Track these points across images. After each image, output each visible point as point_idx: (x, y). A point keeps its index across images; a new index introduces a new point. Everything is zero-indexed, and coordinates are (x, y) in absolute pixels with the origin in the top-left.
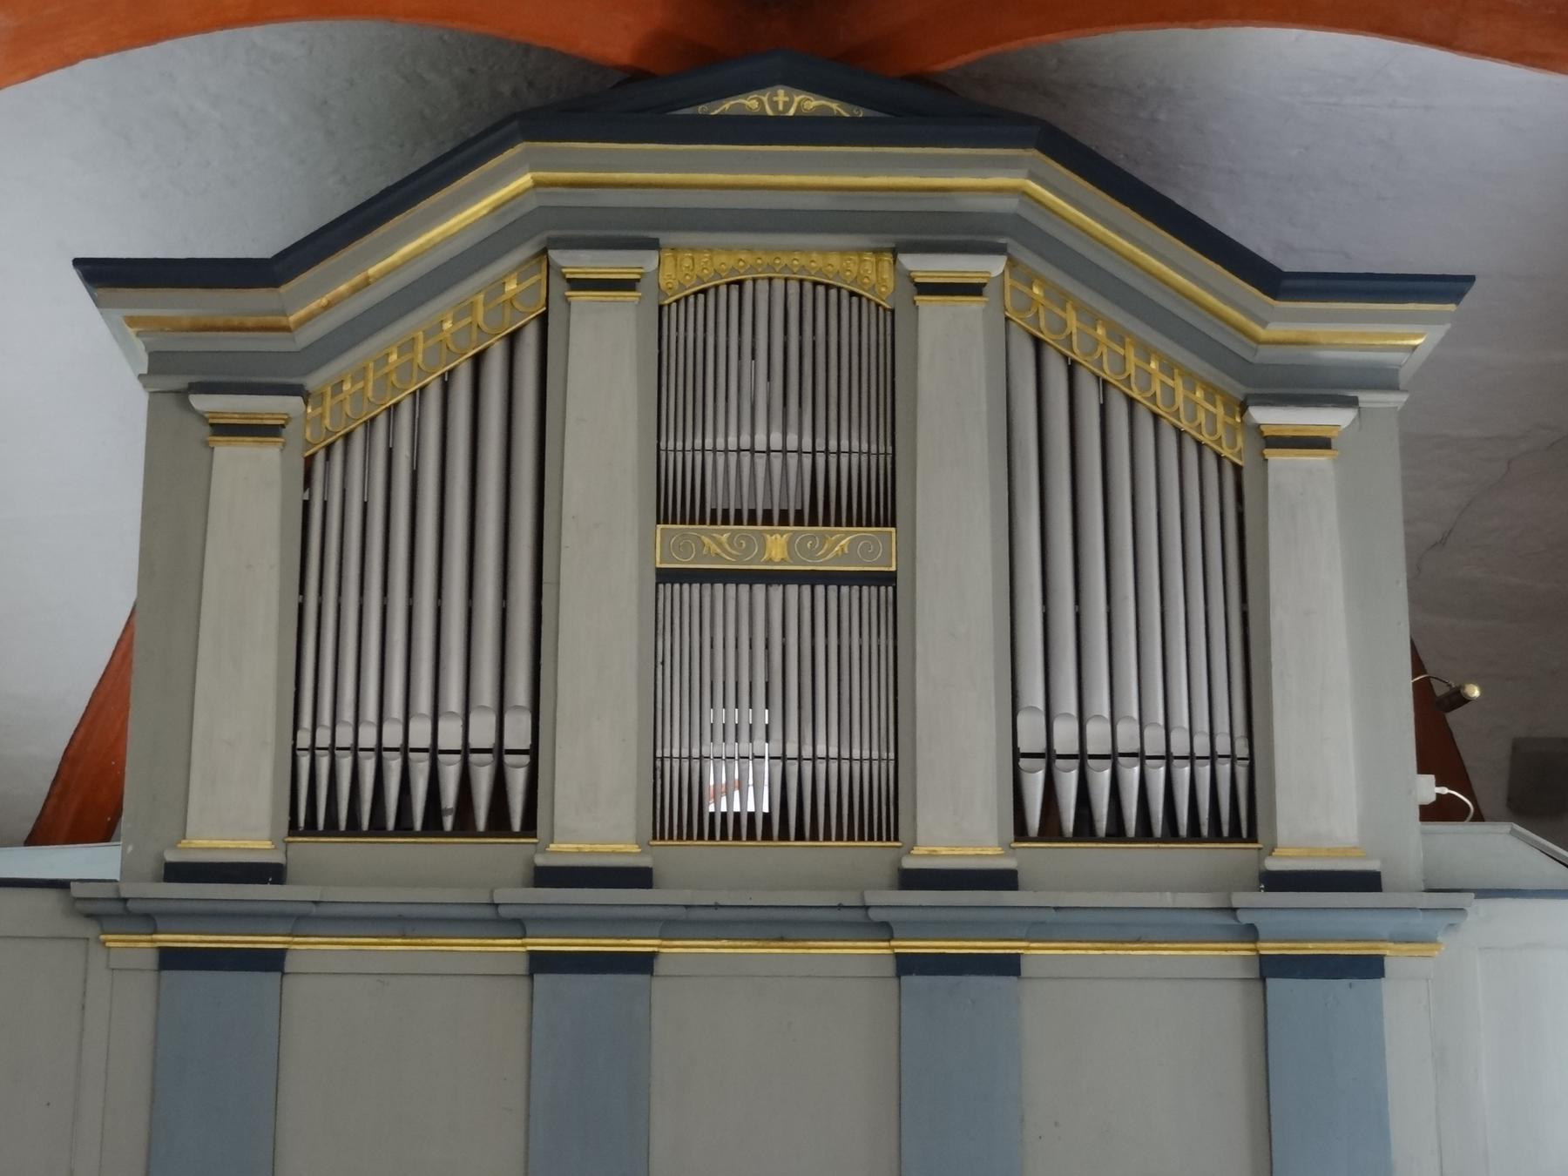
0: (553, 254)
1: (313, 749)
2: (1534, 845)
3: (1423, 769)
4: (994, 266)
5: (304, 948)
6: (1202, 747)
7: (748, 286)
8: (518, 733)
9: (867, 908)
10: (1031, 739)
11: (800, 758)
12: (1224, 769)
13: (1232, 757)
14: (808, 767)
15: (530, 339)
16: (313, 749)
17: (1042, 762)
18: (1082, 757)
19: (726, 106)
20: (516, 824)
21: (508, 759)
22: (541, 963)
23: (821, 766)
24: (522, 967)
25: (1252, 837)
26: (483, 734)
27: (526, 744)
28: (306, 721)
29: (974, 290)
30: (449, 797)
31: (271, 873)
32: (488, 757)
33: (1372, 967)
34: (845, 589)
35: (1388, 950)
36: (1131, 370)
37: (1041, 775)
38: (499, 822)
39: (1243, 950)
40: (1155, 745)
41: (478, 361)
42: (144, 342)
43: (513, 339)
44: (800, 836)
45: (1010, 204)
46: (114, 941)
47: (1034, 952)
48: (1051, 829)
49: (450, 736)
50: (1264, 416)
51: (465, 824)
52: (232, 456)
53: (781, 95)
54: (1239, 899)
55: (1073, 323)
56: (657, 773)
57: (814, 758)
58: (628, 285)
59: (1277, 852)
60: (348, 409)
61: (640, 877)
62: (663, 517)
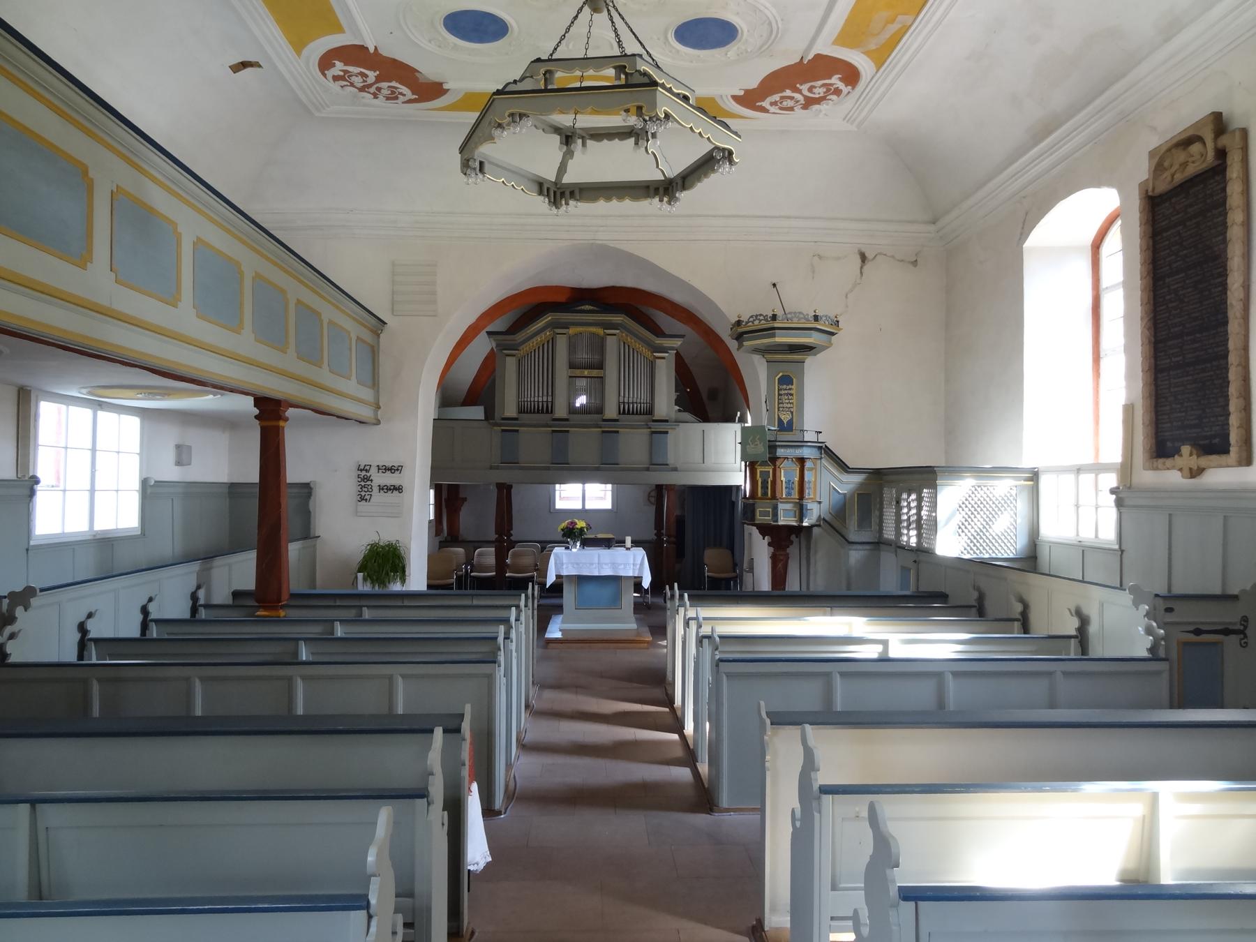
3: (676, 405)
4: (618, 331)
6: (645, 402)
8: (550, 399)
15: (551, 341)
18: (628, 403)
19: (580, 308)
22: (554, 431)
29: (615, 335)
31: (516, 419)
33: (667, 433)
35: (670, 431)
38: (547, 412)
39: (649, 430)
40: (639, 401)
42: (495, 340)
43: (548, 342)
45: (620, 322)
46: (495, 428)
48: (624, 413)
50: (655, 354)
51: (542, 412)
53: (587, 306)
54: (649, 423)
55: (629, 340)
58: (565, 334)
61: (567, 420)
62: (570, 368)
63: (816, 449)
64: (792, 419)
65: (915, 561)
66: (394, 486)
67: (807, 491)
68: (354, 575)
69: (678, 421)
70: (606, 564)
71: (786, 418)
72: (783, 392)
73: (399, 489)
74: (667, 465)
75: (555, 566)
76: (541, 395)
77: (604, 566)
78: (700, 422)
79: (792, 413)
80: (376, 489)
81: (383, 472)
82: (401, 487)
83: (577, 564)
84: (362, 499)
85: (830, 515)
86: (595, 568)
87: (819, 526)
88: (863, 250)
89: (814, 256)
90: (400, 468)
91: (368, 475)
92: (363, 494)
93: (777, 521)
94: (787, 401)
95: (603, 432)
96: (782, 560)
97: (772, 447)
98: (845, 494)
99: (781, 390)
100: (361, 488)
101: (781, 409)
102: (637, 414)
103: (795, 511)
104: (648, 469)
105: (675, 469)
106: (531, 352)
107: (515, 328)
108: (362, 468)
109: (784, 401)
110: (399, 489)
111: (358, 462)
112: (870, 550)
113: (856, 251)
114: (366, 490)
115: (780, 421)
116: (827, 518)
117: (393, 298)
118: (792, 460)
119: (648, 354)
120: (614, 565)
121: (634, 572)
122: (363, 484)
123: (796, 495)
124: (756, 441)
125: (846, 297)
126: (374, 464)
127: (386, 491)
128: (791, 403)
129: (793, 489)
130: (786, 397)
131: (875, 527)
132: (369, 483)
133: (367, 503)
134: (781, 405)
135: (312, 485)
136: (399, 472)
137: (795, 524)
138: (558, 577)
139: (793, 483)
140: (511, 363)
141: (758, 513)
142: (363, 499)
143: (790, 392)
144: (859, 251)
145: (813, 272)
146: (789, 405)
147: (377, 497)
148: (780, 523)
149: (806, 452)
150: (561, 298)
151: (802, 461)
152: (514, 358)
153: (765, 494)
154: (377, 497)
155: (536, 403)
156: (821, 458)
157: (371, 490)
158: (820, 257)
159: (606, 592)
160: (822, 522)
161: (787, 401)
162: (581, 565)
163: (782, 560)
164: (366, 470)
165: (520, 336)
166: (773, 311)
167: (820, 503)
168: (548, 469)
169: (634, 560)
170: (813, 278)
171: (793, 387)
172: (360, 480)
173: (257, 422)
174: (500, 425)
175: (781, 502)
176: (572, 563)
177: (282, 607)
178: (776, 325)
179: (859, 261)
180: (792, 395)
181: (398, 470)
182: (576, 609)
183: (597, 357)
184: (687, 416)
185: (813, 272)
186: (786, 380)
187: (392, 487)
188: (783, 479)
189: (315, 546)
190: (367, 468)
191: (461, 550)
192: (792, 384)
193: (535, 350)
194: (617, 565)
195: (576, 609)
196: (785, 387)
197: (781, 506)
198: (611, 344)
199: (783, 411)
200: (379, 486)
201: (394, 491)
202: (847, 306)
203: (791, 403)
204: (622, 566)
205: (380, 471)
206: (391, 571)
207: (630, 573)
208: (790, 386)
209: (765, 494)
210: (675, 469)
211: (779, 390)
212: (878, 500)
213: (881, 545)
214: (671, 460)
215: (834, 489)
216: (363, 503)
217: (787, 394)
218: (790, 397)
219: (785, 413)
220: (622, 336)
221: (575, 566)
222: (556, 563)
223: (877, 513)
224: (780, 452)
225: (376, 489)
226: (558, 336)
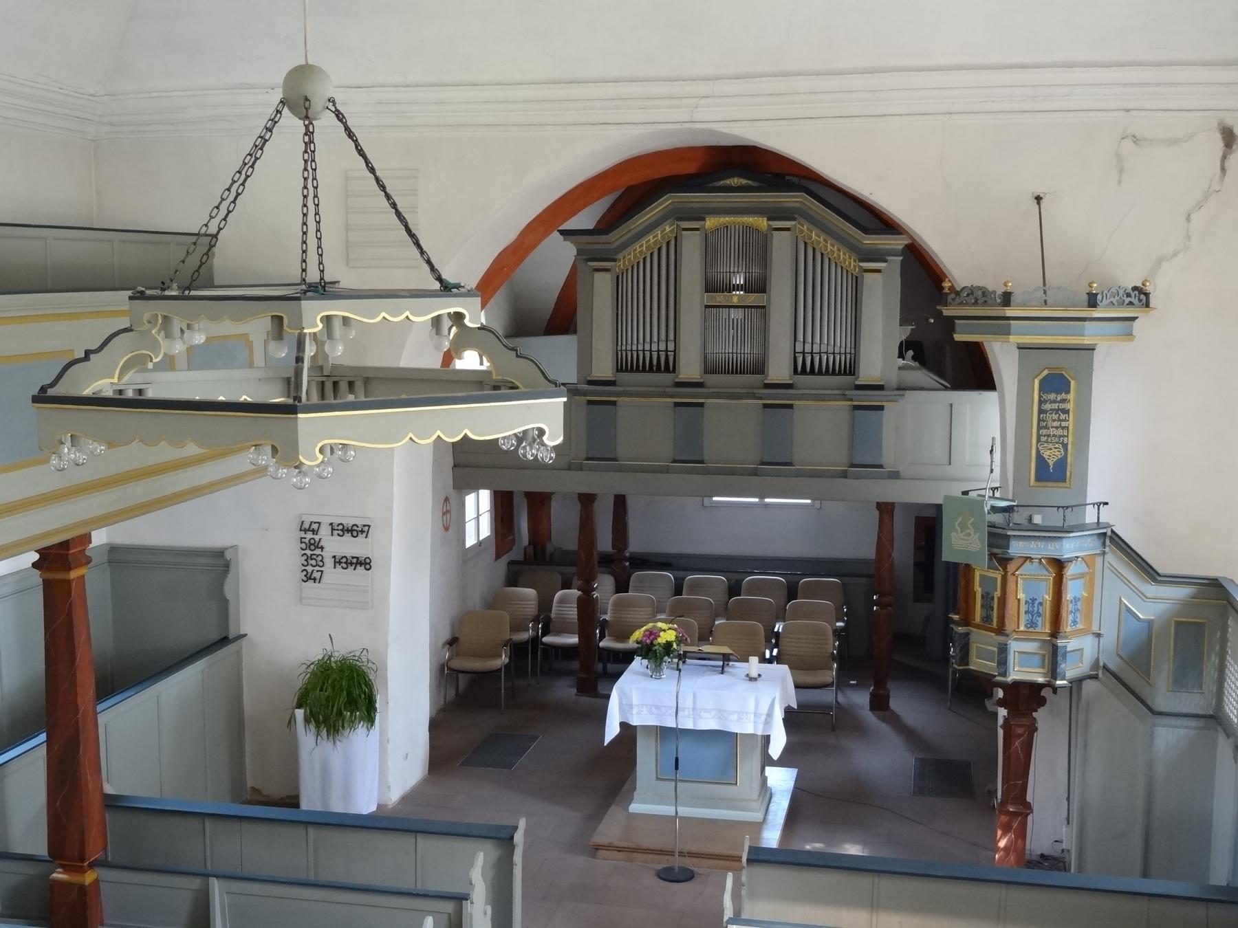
0: (679, 223)
1: (621, 350)
2: (928, 375)
4: (793, 223)
5: (621, 400)
6: (843, 351)
7: (729, 227)
8: (671, 347)
9: (754, 393)
10: (799, 348)
11: (741, 353)
12: (848, 356)
13: (851, 353)
14: (742, 355)
15: (673, 243)
16: (621, 350)
17: (802, 354)
20: (671, 369)
21: (669, 353)
22: (677, 404)
23: (746, 355)
24: (673, 405)
25: (854, 375)
26: (662, 347)
27: (673, 349)
28: (620, 344)
29: (788, 229)
30: (655, 362)
32: (664, 353)
33: (881, 408)
34: (753, 310)
36: (829, 250)
37: (801, 358)
38: (667, 370)
39: (849, 403)
41: (659, 249)
44: (740, 373)
45: (798, 205)
47: (798, 402)
48: (804, 372)
49: (655, 347)
50: (861, 264)
52: (597, 275)
53: (736, 180)
56: (705, 357)
57: (744, 353)
59: (860, 379)
60: (627, 263)
62: (707, 291)
63: (1095, 537)
64: (1065, 458)
66: (357, 558)
67: (1071, 617)
68: (290, 712)
69: (902, 388)
70: (706, 711)
71: (1052, 455)
72: (1048, 406)
73: (366, 564)
74: (881, 466)
75: (620, 708)
76: (655, 339)
77: (704, 715)
78: (946, 388)
79: (1065, 446)
80: (329, 562)
81: (338, 535)
82: (368, 561)
83: (657, 707)
84: (309, 578)
85: (1118, 659)
86: (689, 717)
87: (1095, 677)
88: (1229, 122)
89: (1123, 138)
90: (366, 528)
91: (317, 538)
92: (310, 569)
93: (1004, 674)
94: (1056, 424)
95: (765, 406)
96: (1020, 736)
97: (997, 540)
98: (1150, 623)
99: (1045, 401)
100: (306, 560)
101: (1043, 439)
102: (827, 373)
103: (1044, 656)
104: (844, 475)
105: (895, 475)
106: (638, 263)
107: (607, 224)
108: (306, 526)
109: (1050, 423)
110: (366, 564)
111: (301, 516)
112: (1196, 728)
113: (1215, 125)
114: (313, 562)
115: (1041, 460)
116: (1111, 665)
117: (347, 238)
119: (852, 264)
120: (721, 713)
121: (755, 728)
122: (309, 552)
123: (1044, 627)
125: (1188, 219)
126: (325, 521)
127: (345, 566)
128: (1063, 428)
129: (1039, 615)
130: (1055, 417)
131: (1209, 686)
132: (318, 552)
133: (317, 584)
134: (1044, 432)
135: (228, 555)
136: (364, 534)
137: (1041, 680)
138: (624, 725)
140: (603, 285)
142: (310, 579)
143: (1062, 406)
144: (1219, 124)
145: (1121, 171)
146: (1060, 432)
147: (332, 575)
149: (1068, 548)
150: (690, 168)
151: (1059, 565)
152: (607, 276)
153: (987, 618)
154: (332, 575)
155: (648, 354)
156: (1104, 553)
157: (321, 564)
158: (1136, 140)
159: (711, 754)
160: (1098, 671)
161: (1056, 424)
162: (663, 710)
163: (1020, 736)
164: (313, 531)
165: (617, 236)
166: (1005, 285)
167: (1098, 635)
168: (666, 470)
169: (757, 707)
170: (1120, 182)
171: (1071, 396)
172: (303, 546)
173: (38, 572)
174: (585, 394)
175: (1016, 639)
176: (646, 706)
177: (91, 866)
178: (1010, 312)
179: (1219, 144)
180: (1066, 412)
181: (362, 532)
182: (658, 779)
183: (756, 271)
184: (923, 376)
185: (1121, 171)
186: (1055, 384)
187: (355, 561)
188: (1021, 596)
189: (239, 652)
190: (315, 526)
191: (531, 592)
192: (1068, 392)
193: (632, 267)
194: (725, 715)
195: (658, 779)
196: (1052, 396)
197: (1015, 646)
198: (781, 246)
199: (1047, 442)
200: (334, 557)
201: (358, 567)
202: (1188, 238)
203: (1063, 428)
204: (735, 717)
205: (336, 532)
206: (345, 710)
207: (746, 726)
208: (1064, 396)
209: (987, 618)
210: (895, 475)
211: (1040, 402)
212: (1218, 634)
214: (889, 457)
216: (310, 583)
217: (1057, 411)
218: (1063, 417)
219: (1050, 446)
220: (801, 231)
221: (654, 710)
222: (621, 705)
223: (1215, 660)
224: (1016, 548)
225: (329, 562)
226: (684, 233)
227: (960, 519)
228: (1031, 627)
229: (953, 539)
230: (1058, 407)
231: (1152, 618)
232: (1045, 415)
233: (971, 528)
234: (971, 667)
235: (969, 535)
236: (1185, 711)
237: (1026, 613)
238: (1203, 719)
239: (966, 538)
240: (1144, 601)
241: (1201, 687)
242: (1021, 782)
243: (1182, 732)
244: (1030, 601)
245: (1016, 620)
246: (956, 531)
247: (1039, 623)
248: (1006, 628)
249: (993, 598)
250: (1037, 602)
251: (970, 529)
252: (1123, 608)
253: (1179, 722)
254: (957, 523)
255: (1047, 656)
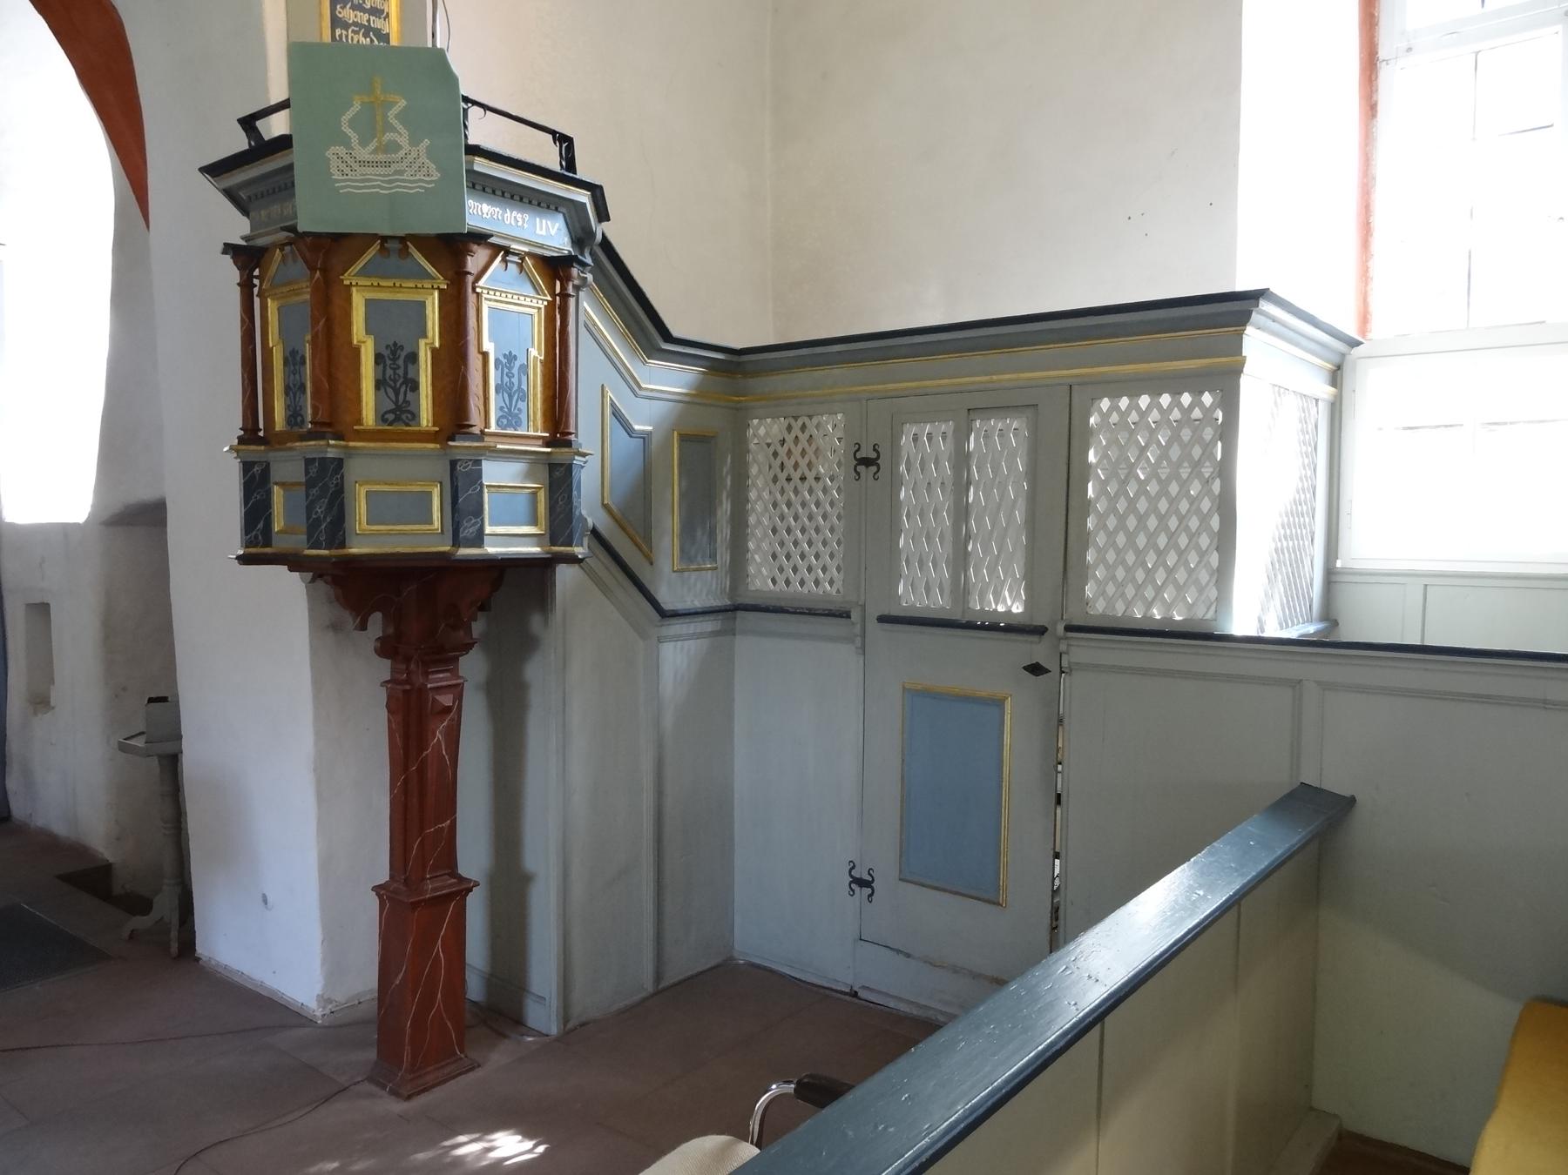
65: (1036, 669)
93: (479, 539)
96: (448, 710)
98: (645, 438)
103: (534, 494)
112: (715, 634)
116: (601, 529)
118: (521, 266)
123: (533, 425)
124: (389, 128)
131: (724, 556)
139: (524, 369)
141: (360, 509)
143: (377, 23)
148: (492, 549)
153: (399, 412)
188: (488, 346)
209: (399, 412)
213: (740, 614)
215: (616, 413)
227: (357, 107)
228: (509, 425)
229: (334, 163)
230: (369, 21)
231: (650, 428)
232: (344, 32)
233: (400, 127)
234: (354, 551)
235: (395, 147)
236: (698, 604)
237: (497, 391)
238: (720, 616)
239: (381, 157)
240: (636, 395)
241: (713, 557)
242: (449, 821)
243: (692, 645)
244: (504, 361)
245: (482, 407)
246: (346, 143)
247: (523, 417)
248: (472, 422)
249: (413, 358)
250: (517, 364)
251: (394, 130)
252: (608, 411)
253: (712, 617)
254: (346, 118)
255: (542, 496)
